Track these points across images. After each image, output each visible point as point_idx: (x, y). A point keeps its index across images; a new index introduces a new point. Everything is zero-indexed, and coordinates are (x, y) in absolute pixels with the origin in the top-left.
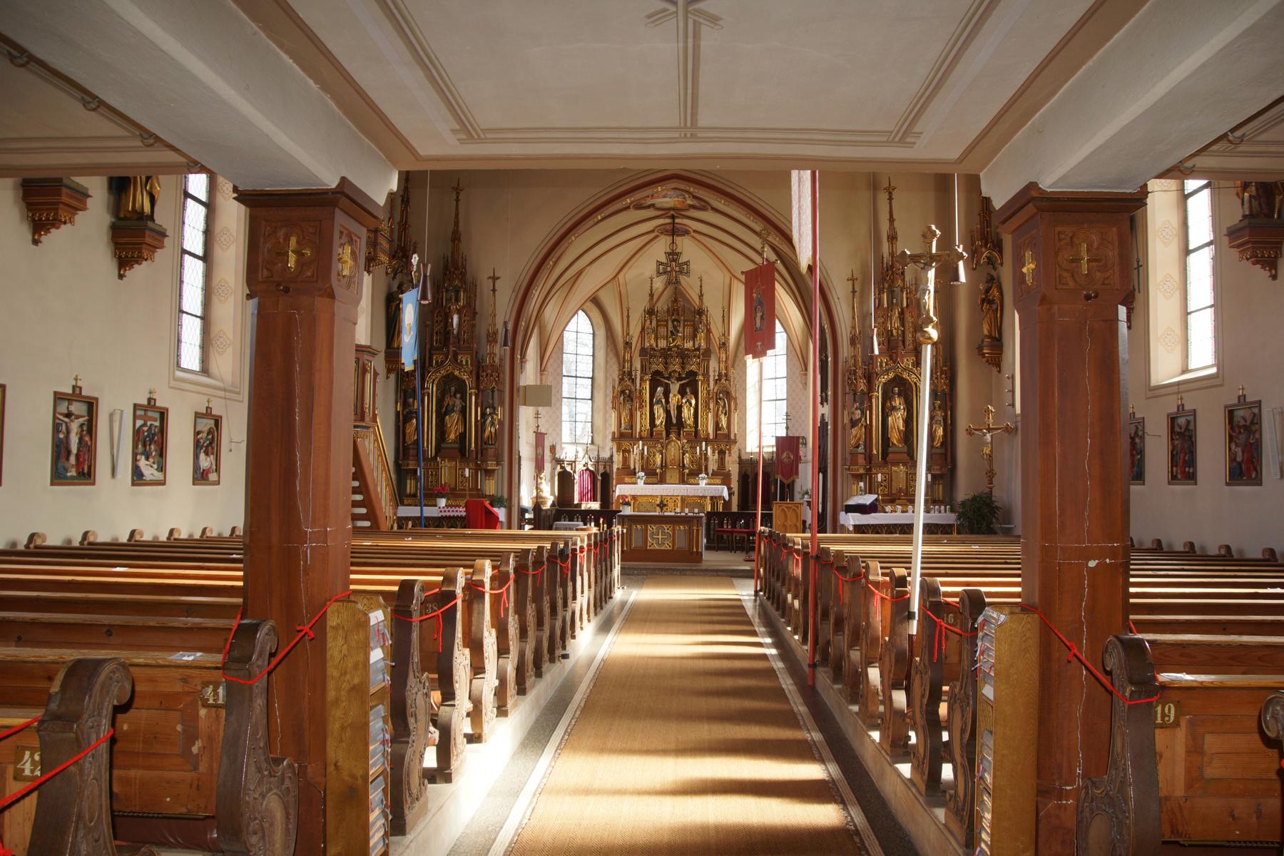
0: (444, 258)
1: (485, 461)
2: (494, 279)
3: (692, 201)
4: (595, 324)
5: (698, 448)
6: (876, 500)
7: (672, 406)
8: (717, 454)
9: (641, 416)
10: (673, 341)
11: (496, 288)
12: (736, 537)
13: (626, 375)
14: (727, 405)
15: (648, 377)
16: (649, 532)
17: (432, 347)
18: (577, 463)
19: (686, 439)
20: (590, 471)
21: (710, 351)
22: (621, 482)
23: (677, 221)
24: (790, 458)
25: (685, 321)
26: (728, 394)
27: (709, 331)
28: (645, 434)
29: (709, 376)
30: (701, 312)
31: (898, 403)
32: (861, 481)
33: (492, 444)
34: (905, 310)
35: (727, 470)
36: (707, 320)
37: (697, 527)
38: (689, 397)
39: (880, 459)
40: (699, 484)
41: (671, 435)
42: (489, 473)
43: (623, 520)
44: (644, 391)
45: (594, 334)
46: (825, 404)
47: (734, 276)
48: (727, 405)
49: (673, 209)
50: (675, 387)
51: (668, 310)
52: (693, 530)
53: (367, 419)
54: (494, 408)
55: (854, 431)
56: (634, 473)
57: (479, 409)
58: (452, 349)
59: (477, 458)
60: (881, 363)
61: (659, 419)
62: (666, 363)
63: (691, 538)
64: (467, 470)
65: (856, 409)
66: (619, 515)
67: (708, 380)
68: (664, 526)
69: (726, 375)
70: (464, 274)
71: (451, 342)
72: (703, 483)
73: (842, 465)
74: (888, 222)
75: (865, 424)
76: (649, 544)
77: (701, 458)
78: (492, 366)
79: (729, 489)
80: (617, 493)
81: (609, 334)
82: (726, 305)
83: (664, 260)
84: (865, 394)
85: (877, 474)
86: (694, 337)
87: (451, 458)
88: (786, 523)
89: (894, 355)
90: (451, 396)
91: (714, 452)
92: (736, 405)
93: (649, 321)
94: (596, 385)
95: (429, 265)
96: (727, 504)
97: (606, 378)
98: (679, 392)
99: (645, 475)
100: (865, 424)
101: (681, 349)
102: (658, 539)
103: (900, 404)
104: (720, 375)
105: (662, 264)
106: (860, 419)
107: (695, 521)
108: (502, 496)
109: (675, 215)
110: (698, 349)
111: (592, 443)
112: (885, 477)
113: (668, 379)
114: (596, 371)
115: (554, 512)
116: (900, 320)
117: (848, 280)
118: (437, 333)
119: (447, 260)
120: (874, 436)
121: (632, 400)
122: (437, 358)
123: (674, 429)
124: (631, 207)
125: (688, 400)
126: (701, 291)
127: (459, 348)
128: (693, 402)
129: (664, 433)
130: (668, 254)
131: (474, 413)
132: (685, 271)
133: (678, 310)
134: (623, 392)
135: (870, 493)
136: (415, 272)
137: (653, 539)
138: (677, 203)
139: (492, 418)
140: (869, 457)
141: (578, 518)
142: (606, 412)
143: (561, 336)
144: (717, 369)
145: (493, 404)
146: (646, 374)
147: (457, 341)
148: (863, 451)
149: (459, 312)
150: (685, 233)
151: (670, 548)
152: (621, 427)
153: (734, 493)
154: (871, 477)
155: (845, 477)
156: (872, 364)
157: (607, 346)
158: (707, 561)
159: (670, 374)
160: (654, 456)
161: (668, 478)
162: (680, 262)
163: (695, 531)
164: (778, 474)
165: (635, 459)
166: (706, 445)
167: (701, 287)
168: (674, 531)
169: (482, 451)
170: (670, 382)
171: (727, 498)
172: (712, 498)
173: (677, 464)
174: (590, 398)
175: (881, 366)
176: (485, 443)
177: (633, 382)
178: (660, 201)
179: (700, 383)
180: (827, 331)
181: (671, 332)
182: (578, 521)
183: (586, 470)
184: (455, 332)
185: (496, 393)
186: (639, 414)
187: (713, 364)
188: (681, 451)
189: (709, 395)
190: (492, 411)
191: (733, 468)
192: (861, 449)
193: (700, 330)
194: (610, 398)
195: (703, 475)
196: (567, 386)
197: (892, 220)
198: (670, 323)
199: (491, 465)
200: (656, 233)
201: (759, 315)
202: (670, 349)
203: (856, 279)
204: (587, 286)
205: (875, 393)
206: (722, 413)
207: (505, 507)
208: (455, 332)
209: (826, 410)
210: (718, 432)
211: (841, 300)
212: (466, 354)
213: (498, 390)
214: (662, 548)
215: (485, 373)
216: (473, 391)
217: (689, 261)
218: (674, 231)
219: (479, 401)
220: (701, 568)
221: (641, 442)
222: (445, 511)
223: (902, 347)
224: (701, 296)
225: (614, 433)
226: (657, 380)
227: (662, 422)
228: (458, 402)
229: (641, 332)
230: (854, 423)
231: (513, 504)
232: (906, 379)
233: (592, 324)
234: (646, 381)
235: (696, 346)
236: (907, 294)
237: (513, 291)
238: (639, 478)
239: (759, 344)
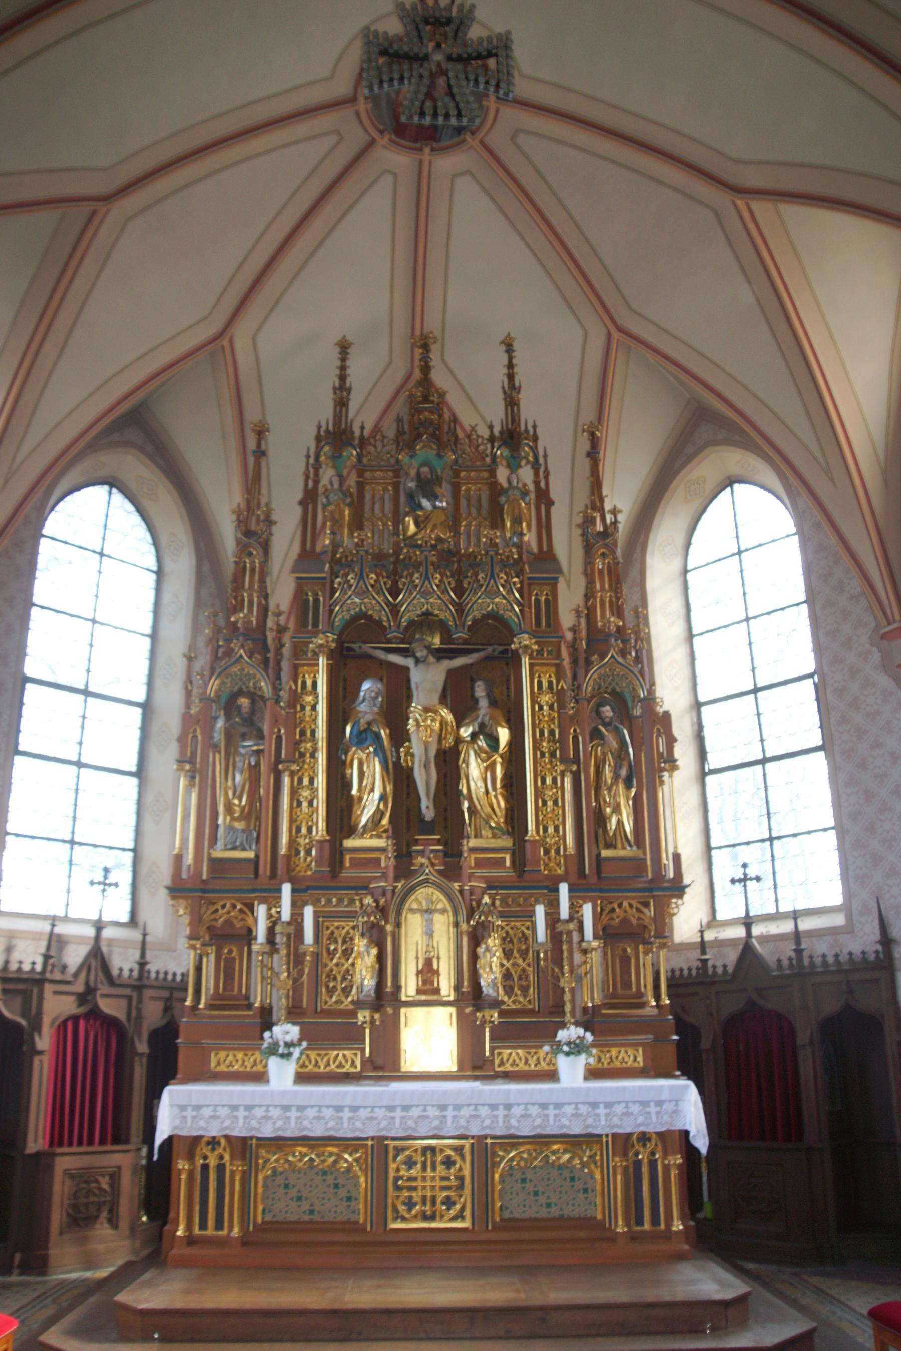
4: (164, 540)
5: (540, 911)
7: (417, 747)
9: (294, 792)
15: (324, 640)
18: (48, 988)
27: (544, 498)
40: (552, 1076)
44: (309, 698)
47: (620, 329)
51: (400, 433)
56: (266, 1021)
81: (206, 567)
93: (328, 475)
98: (443, 700)
111: (133, 921)
114: (158, 683)
121: (260, 736)
125: (482, 726)
126: (511, 377)
128: (503, 734)
152: (214, 840)
157: (198, 604)
160: (347, 953)
174: (134, 769)
177: (265, 662)
179: (525, 662)
183: (88, 1016)
195: (570, 1033)
206: (616, 776)
210: (605, 853)
227: (379, 815)
229: (303, 503)
233: (156, 543)
234: (316, 655)
238: (273, 1050)
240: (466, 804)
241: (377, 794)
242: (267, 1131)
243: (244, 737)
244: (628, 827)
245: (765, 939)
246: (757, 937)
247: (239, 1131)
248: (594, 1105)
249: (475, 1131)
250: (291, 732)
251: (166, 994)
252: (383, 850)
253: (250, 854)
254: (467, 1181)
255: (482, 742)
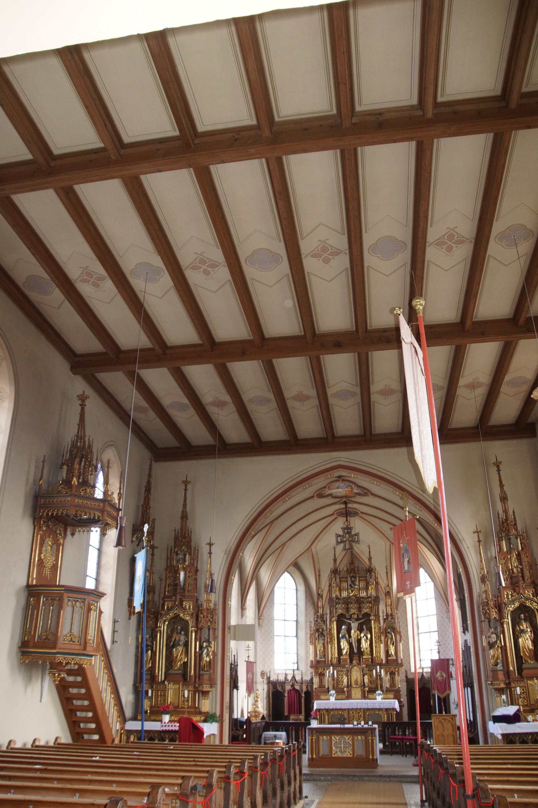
0: (175, 531)
1: (201, 684)
2: (210, 545)
3: (357, 490)
4: (297, 582)
5: (374, 671)
6: (519, 710)
8: (389, 675)
9: (331, 648)
10: (352, 592)
11: (212, 552)
12: (406, 743)
13: (320, 619)
14: (394, 637)
16: (333, 743)
17: (165, 597)
18: (286, 684)
19: (365, 664)
20: (297, 690)
21: (379, 598)
22: (318, 699)
23: (350, 505)
24: (443, 676)
25: (359, 577)
26: (394, 629)
27: (377, 583)
28: (335, 661)
29: (380, 616)
30: (370, 570)
31: (525, 626)
32: (503, 694)
33: (207, 671)
34: (521, 553)
35: (397, 688)
36: (375, 576)
37: (372, 737)
38: (365, 632)
39: (517, 675)
40: (376, 699)
41: (354, 662)
42: (205, 694)
43: (312, 732)
45: (297, 589)
46: (466, 632)
48: (394, 637)
49: (346, 497)
50: (354, 625)
51: (347, 570)
52: (369, 739)
53: (88, 648)
54: (209, 642)
55: (492, 652)
56: (328, 691)
57: (198, 643)
58: (178, 596)
59: (195, 682)
60: (507, 595)
61: (344, 649)
62: (348, 608)
63: (369, 747)
64: (186, 692)
65: (492, 633)
66: (310, 729)
67: (379, 619)
68: (345, 737)
69: (391, 615)
70: (190, 541)
71: (178, 591)
72: (379, 698)
73: (486, 681)
74: (499, 487)
75: (500, 645)
76: (333, 752)
77: (377, 679)
78: (207, 609)
79: (400, 702)
80: (315, 707)
81: (307, 589)
82: (388, 565)
83: (341, 533)
84: (497, 621)
85: (516, 687)
86: (367, 589)
87: (176, 682)
88: (444, 734)
89: (517, 588)
90: (177, 633)
91: (386, 674)
92: (401, 637)
93: (334, 579)
94: (299, 626)
95: (125, 518)
96: (399, 715)
97: (306, 621)
98: (358, 629)
99: (336, 692)
100: (500, 645)
101: (358, 597)
102: (341, 747)
103: (527, 627)
104: (387, 615)
105: (339, 536)
106: (496, 642)
107: (370, 732)
108: (215, 713)
109: (347, 501)
110: (370, 597)
111: (298, 669)
112: (523, 690)
113: (350, 619)
114: (299, 616)
115: (263, 724)
116: (518, 561)
117: (474, 533)
118: (168, 586)
119: (178, 533)
120: (509, 655)
121: (324, 636)
122: (168, 604)
123: (356, 657)
124: (315, 495)
125: (365, 635)
127: (184, 597)
128: (369, 636)
129: (348, 661)
130: (343, 529)
131: (194, 646)
132: (356, 540)
133: (354, 569)
134: (317, 630)
135: (512, 704)
136: (145, 538)
137: (336, 747)
138: (347, 492)
139: (208, 650)
140: (507, 673)
141: (282, 728)
142: (307, 646)
143: (273, 591)
144: (385, 611)
145: (209, 639)
146: (333, 617)
147: (183, 591)
148: (502, 668)
149: (184, 569)
150: (355, 513)
151: (351, 756)
153: (403, 706)
154: (511, 690)
155: (489, 689)
156: (501, 596)
158: (381, 766)
159: (351, 616)
160: (342, 678)
161: (353, 695)
162: (353, 533)
163: (370, 740)
164: (435, 690)
165: (328, 681)
166: (380, 669)
167: (370, 552)
168: (353, 740)
169: (199, 676)
170: (351, 622)
171: (398, 710)
172: (387, 710)
173: (359, 683)
175: (508, 597)
176: (202, 670)
178: (335, 491)
179: (373, 622)
180: (462, 573)
181: (351, 585)
182: (282, 731)
184: (182, 584)
185: (211, 631)
186: (330, 646)
187: (382, 607)
188: (362, 674)
189: (380, 630)
190: (207, 644)
191: (402, 685)
192: (500, 667)
193: (371, 583)
194: (308, 636)
195: (379, 692)
196: (279, 627)
197: (501, 485)
198: (349, 579)
199: (206, 688)
200: (335, 516)
201: (406, 560)
202: (349, 597)
203: (480, 532)
204: (290, 555)
205: (506, 620)
206: (390, 642)
207: (216, 721)
208: (182, 584)
209: (469, 636)
210: (389, 658)
211: (470, 549)
212: (190, 600)
213: (212, 628)
214: (345, 755)
215: (202, 615)
216: (193, 629)
217: (358, 533)
218: (347, 514)
219: (198, 637)
220: (376, 774)
221: (331, 668)
222: (169, 726)
223: (523, 582)
224: (370, 559)
225: (312, 662)
226: (341, 620)
227: (347, 652)
228: (183, 638)
229: (329, 586)
230: (491, 646)
231: (224, 719)
232: (529, 607)
233: (295, 582)
235: (369, 595)
236: (520, 540)
237: (225, 554)
238: (331, 695)
239: (408, 583)
240: (362, 650)
241: (346, 649)
242: (331, 708)
243: (321, 637)
244: (393, 653)
245: (426, 673)
246: (425, 673)
247: (327, 708)
248: (381, 704)
249: (363, 707)
250: (330, 637)
251: (306, 684)
252: (347, 659)
253: (324, 659)
254: (362, 716)
255: (365, 637)
